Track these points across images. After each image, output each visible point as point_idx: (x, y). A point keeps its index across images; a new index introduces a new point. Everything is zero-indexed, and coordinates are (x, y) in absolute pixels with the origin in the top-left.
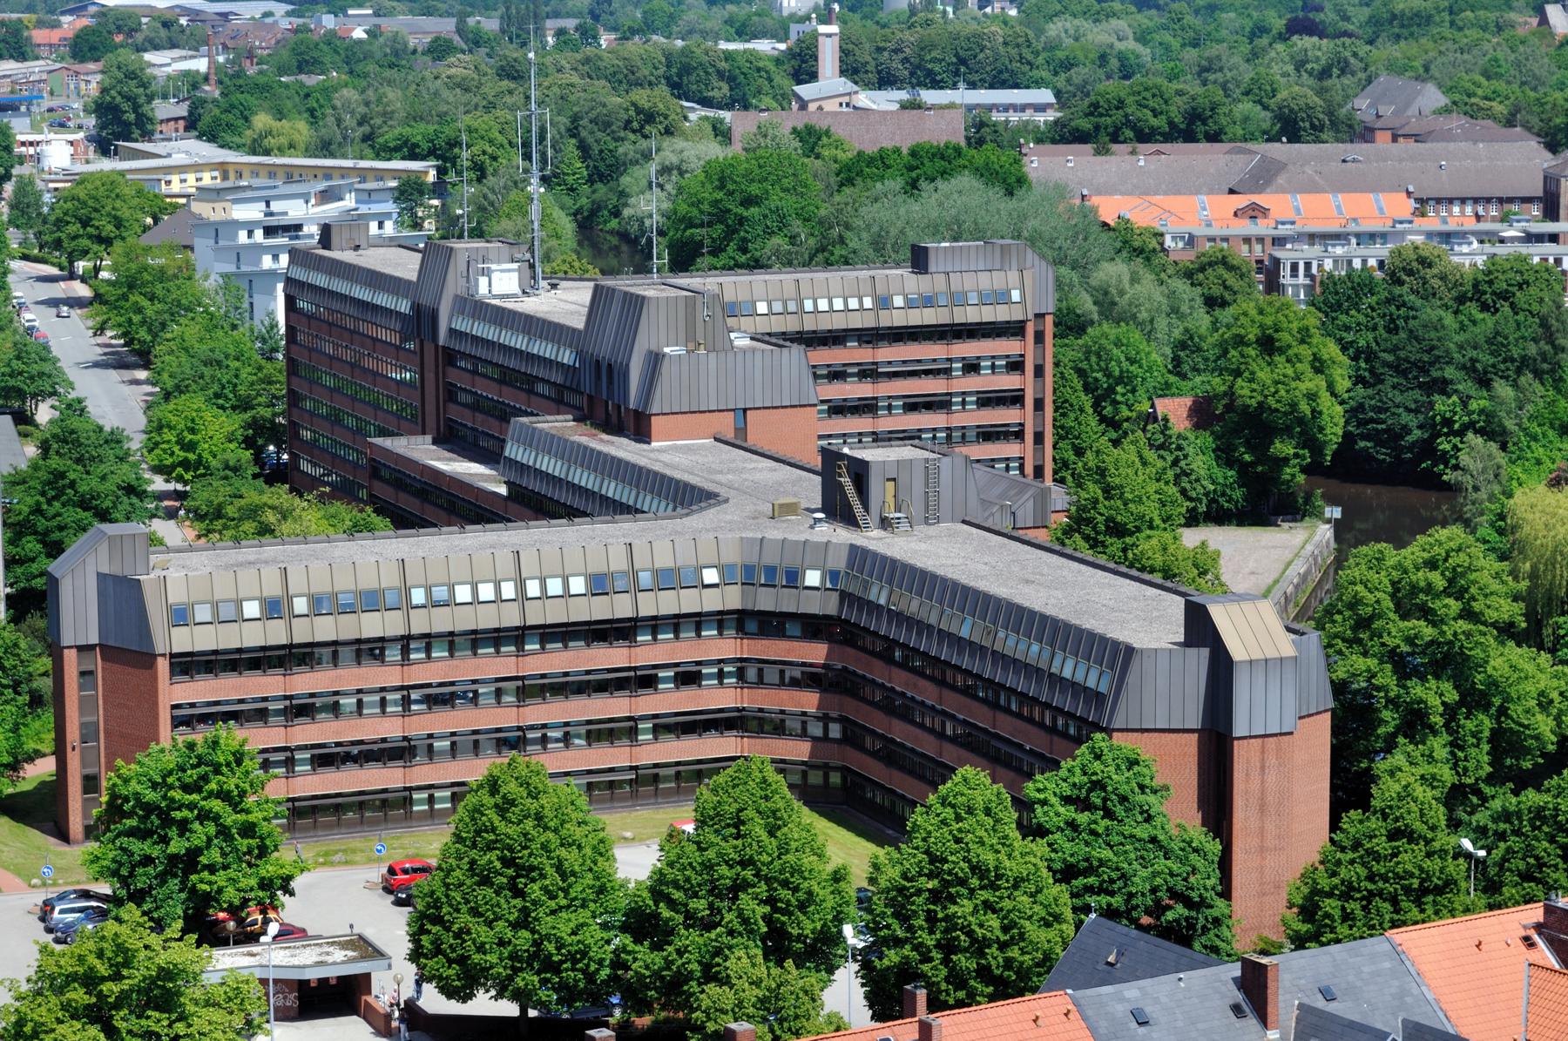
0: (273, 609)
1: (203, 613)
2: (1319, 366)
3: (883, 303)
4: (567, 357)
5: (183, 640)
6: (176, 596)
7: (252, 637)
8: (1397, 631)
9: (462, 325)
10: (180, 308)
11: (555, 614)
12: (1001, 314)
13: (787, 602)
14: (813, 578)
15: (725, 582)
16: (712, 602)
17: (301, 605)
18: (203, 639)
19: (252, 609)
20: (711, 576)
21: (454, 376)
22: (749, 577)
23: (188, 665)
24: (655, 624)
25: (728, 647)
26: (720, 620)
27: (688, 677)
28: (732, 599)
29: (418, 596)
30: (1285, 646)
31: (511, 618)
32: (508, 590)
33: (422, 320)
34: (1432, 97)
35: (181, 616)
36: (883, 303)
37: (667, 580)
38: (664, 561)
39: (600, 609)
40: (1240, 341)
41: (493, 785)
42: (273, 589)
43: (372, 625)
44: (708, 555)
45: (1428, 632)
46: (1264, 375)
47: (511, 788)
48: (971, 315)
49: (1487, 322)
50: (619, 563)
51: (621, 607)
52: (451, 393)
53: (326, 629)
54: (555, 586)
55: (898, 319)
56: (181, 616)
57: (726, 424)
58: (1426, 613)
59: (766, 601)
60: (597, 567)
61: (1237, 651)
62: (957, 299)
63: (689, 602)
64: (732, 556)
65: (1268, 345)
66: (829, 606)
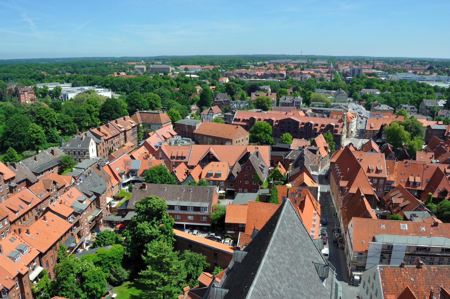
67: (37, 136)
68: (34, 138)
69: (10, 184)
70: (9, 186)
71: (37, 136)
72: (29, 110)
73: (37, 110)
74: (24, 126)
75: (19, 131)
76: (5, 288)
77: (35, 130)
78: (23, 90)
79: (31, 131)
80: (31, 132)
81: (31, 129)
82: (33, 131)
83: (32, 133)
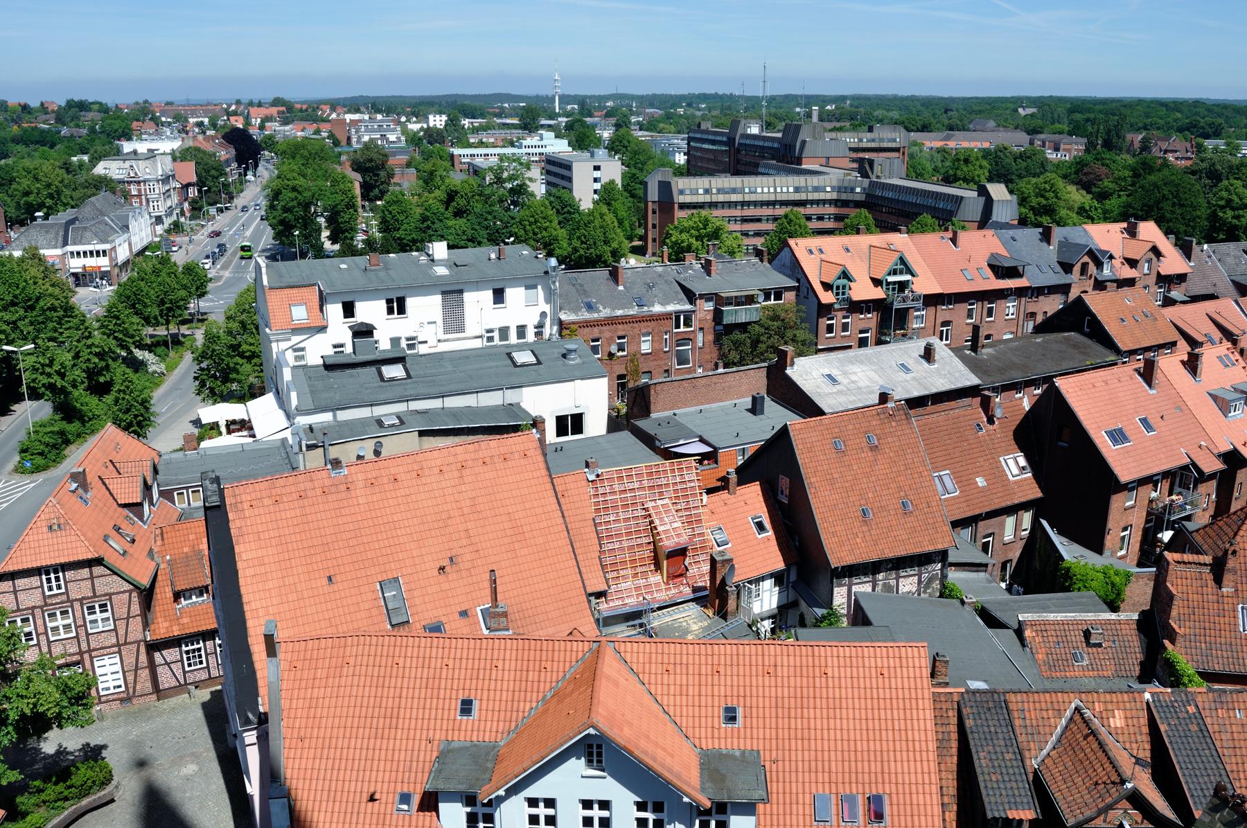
0: (707, 191)
1: (687, 192)
2: (981, 167)
3: (861, 140)
4: (776, 145)
5: (682, 199)
6: (680, 187)
7: (701, 199)
8: (1034, 201)
9: (743, 141)
10: (650, 158)
11: (785, 197)
12: (893, 145)
13: (850, 197)
14: (858, 190)
15: (833, 190)
16: (828, 196)
17: (714, 191)
18: (687, 199)
19: (701, 191)
20: (828, 189)
21: (739, 157)
22: (839, 190)
23: (683, 206)
24: (812, 202)
25: (831, 210)
26: (830, 202)
27: (820, 218)
28: (834, 196)
29: (747, 190)
30: (1008, 196)
31: (772, 198)
32: (772, 190)
33: (731, 141)
34: (992, 124)
35: (681, 192)
36: (861, 140)
37: (816, 189)
38: (815, 184)
39: (797, 197)
40: (958, 160)
41: (786, 216)
42: (707, 186)
43: (734, 198)
44: (828, 183)
45: (1044, 202)
46: (965, 169)
47: (792, 217)
48: (885, 145)
49: (1024, 164)
50: (803, 184)
51: (803, 197)
52: (738, 161)
53: (721, 198)
54: (785, 190)
55: (864, 145)
56: (681, 192)
57: (823, 161)
58: (1042, 196)
59: (844, 197)
60: (797, 185)
61: (994, 198)
62: (882, 140)
63: (822, 196)
64: (835, 183)
65: (966, 161)
66: (863, 198)
67: (1238, 217)
68: (1224, 223)
69: (1169, 291)
70: (1165, 297)
71: (1238, 217)
72: (1204, 165)
73: (1231, 167)
74: (1182, 206)
75: (1168, 215)
76: (1194, 464)
77: (1235, 198)
78: (1164, 146)
79: (1222, 199)
80: (1222, 203)
81: (1224, 194)
82: (1229, 201)
83: (1222, 207)
